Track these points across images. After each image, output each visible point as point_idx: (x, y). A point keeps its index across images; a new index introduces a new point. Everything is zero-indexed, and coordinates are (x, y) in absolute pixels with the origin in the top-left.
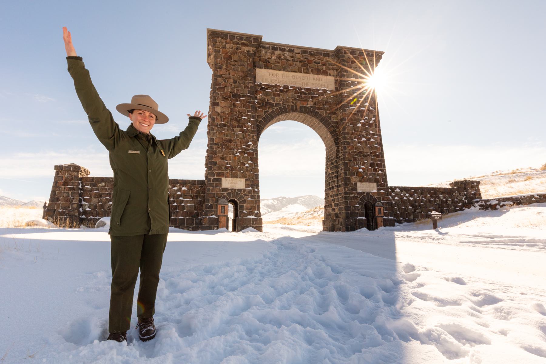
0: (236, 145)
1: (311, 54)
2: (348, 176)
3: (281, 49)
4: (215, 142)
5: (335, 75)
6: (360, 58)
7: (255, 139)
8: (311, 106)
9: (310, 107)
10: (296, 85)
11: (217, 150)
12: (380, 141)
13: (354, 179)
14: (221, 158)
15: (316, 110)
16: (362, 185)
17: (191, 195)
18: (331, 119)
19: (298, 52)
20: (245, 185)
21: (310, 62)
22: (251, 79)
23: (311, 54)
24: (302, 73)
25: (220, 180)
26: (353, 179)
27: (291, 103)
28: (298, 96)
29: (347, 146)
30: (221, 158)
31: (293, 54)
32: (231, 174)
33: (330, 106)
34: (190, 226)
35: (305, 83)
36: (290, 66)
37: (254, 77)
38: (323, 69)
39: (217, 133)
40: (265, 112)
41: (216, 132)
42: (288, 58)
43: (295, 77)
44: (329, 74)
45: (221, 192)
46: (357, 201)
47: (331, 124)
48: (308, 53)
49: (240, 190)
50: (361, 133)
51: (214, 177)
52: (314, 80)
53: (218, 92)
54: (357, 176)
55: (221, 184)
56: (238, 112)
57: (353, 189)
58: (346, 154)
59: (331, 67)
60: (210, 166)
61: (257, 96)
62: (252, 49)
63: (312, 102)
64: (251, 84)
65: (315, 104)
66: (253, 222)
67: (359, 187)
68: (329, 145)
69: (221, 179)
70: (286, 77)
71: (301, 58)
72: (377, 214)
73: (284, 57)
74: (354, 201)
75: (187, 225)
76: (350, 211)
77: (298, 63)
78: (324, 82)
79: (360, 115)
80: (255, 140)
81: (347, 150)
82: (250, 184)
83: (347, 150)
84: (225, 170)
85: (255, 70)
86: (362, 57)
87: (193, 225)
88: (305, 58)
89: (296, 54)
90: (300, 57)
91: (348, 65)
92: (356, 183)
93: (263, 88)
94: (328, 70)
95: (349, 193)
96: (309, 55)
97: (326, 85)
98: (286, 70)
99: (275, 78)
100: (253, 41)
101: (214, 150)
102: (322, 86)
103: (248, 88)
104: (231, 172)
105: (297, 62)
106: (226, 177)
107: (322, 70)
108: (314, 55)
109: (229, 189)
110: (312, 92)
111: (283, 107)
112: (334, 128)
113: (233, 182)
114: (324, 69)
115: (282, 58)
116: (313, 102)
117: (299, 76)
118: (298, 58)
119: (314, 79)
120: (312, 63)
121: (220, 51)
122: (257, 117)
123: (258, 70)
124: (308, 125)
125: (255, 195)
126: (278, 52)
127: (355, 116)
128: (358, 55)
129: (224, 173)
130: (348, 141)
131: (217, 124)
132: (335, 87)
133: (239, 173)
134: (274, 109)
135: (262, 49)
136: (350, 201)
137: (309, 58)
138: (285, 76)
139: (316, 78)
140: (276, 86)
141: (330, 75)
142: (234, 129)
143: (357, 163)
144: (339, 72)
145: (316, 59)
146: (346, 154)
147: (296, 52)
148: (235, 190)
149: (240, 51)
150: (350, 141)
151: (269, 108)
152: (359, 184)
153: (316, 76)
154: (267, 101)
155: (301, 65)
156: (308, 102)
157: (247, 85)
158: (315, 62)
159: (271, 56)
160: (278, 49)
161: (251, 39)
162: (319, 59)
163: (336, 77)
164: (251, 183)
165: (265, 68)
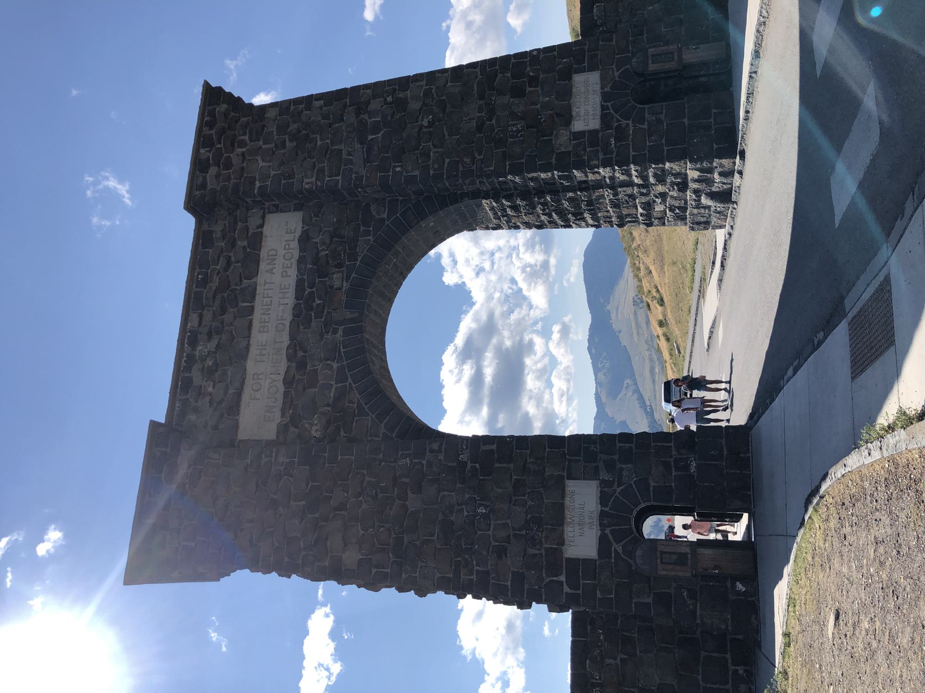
0: (459, 508)
1: (204, 283)
2: (553, 161)
3: (188, 369)
4: (451, 575)
5: (262, 211)
6: (219, 146)
7: (440, 447)
8: (345, 277)
9: (347, 282)
10: (284, 322)
11: (476, 568)
12: (444, 74)
13: (562, 140)
14: (500, 557)
15: (358, 263)
16: (578, 115)
17: (622, 660)
18: (383, 220)
20: (588, 479)
23: (204, 283)
24: (253, 308)
25: (574, 563)
26: (561, 145)
27: (338, 335)
29: (461, 169)
30: (500, 557)
31: (201, 333)
32: (549, 527)
34: (730, 673)
35: (281, 295)
36: (235, 341)
38: (244, 247)
39: (421, 567)
41: (418, 570)
42: (212, 345)
43: (264, 327)
44: (260, 230)
45: (613, 560)
46: (631, 128)
47: (397, 217)
48: (200, 290)
49: (604, 499)
50: (425, 130)
51: (563, 582)
52: (274, 271)
53: (301, 557)
54: (551, 134)
55: (584, 560)
58: (485, 169)
59: (240, 224)
60: (525, 595)
61: (315, 437)
65: (340, 266)
68: (457, 222)
69: (569, 560)
70: (263, 352)
71: (214, 308)
72: (672, 65)
73: (208, 359)
75: (727, 683)
76: (666, 148)
77: (227, 317)
79: (374, 137)
80: (443, 446)
81: (474, 168)
82: (584, 464)
84: (538, 547)
85: (241, 441)
88: (214, 298)
89: (204, 323)
91: (235, 179)
92: (574, 133)
96: (207, 287)
97: (291, 237)
101: (475, 579)
102: (289, 249)
104: (545, 527)
105: (223, 319)
106: (563, 544)
107: (248, 250)
109: (599, 533)
110: (305, 277)
111: (346, 361)
113: (576, 520)
115: (210, 363)
116: (333, 274)
117: (262, 314)
118: (214, 317)
119: (271, 271)
120: (228, 276)
122: (374, 438)
123: (243, 435)
124: (399, 285)
125: (620, 446)
126: (197, 377)
127: (376, 148)
128: (211, 150)
129: (547, 550)
130: (446, 166)
132: (295, 210)
133: (549, 501)
134: (354, 386)
136: (631, 148)
137: (214, 288)
138: (261, 355)
139: (267, 264)
140: (288, 382)
141: (262, 226)
142: (409, 512)
144: (252, 201)
145: (218, 267)
147: (196, 324)
148: (602, 515)
150: (447, 161)
152: (578, 126)
153: (263, 266)
154: (329, 409)
156: (335, 287)
158: (226, 270)
162: (219, 260)
163: (267, 211)
164: (579, 461)
165: (238, 414)
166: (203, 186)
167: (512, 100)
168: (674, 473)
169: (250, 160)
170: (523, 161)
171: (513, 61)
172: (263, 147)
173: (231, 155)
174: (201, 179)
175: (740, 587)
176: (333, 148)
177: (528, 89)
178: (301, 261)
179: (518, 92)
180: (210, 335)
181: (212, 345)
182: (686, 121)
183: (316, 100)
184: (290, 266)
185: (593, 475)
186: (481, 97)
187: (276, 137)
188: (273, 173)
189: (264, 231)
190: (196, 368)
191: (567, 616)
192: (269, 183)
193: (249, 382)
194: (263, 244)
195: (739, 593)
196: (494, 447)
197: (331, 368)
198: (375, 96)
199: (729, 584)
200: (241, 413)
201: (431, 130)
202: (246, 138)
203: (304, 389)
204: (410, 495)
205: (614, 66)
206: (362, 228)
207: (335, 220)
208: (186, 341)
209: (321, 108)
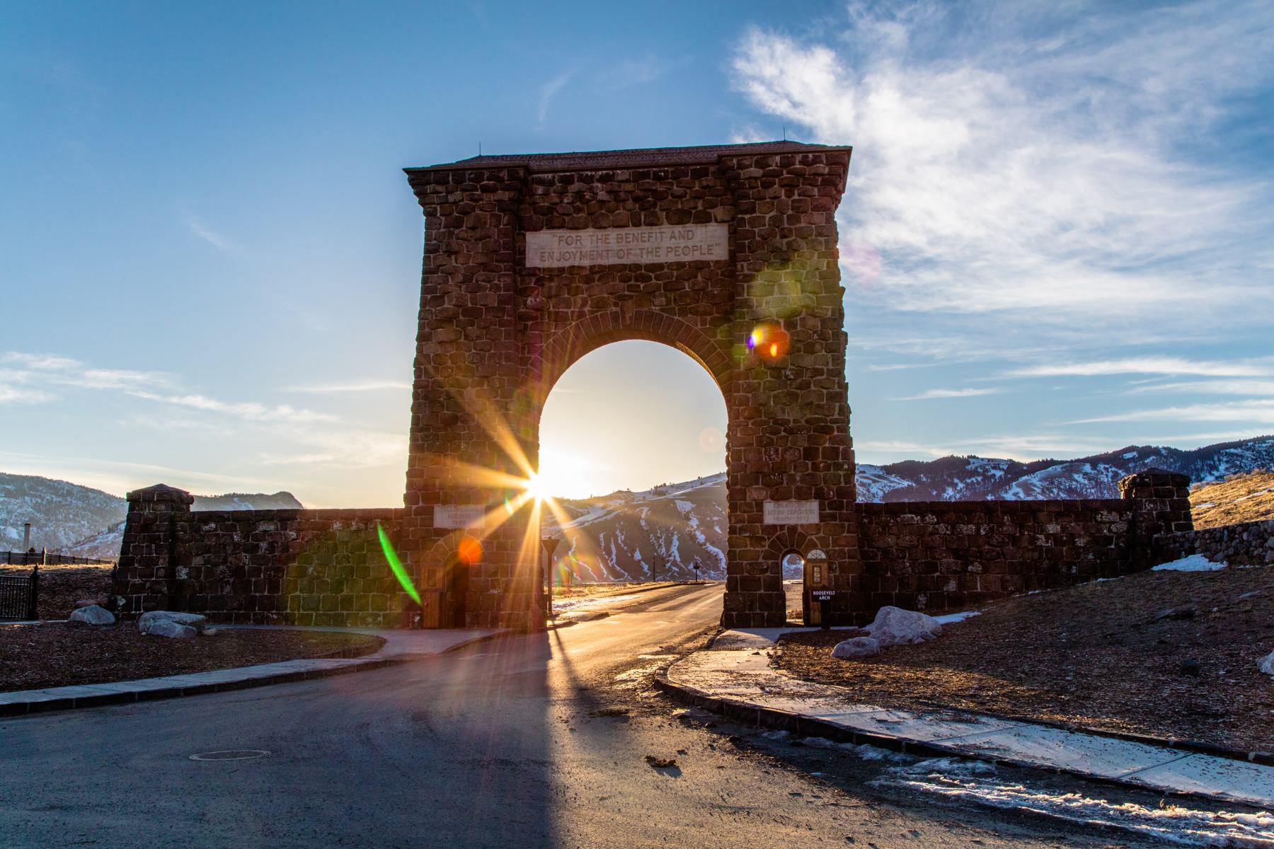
3: (581, 179)
5: (726, 218)
6: (785, 172)
9: (660, 310)
12: (836, 386)
13: (754, 494)
16: (779, 506)
21: (659, 196)
22: (505, 266)
23: (657, 178)
28: (628, 286)
29: (741, 408)
33: (712, 302)
37: (523, 252)
38: (695, 208)
42: (602, 195)
44: (713, 218)
46: (760, 549)
50: (783, 372)
51: (417, 503)
52: (673, 240)
56: (473, 351)
58: (739, 429)
62: (505, 196)
63: (664, 299)
69: (433, 508)
74: (752, 549)
76: (738, 576)
77: (630, 204)
78: (700, 241)
83: (741, 419)
85: (524, 236)
86: (788, 169)
87: (385, 610)
89: (623, 184)
90: (632, 189)
92: (762, 503)
94: (712, 208)
95: (740, 529)
97: (705, 247)
98: (598, 225)
99: (572, 249)
100: (506, 178)
103: (498, 288)
108: (666, 177)
110: (666, 270)
112: (724, 359)
114: (700, 208)
115: (587, 197)
120: (666, 198)
121: (435, 208)
131: (425, 383)
132: (730, 251)
135: (535, 186)
141: (716, 221)
143: (765, 452)
145: (675, 188)
146: (739, 429)
147: (620, 178)
149: (481, 202)
151: (556, 326)
152: (769, 506)
155: (637, 206)
157: (496, 282)
158: (672, 195)
159: (560, 197)
160: (576, 179)
161: (501, 175)
165: (548, 229)
166: (741, 167)
167: (802, 449)
168: (490, 579)
169: (773, 204)
170: (743, 462)
171: (841, 447)
172: (785, 216)
173: (776, 186)
174: (747, 162)
175: (417, 618)
176: (776, 287)
177: (810, 463)
178: (680, 265)
180: (610, 192)
181: (602, 195)
182: (762, 591)
183: (828, 264)
184: (677, 253)
186: (807, 421)
187: (793, 227)
188: (756, 230)
189: (711, 224)
191: (402, 505)
192: (747, 228)
193: (574, 234)
194: (699, 225)
195: (413, 618)
199: (418, 612)
200: (548, 231)
201: (783, 378)
202: (796, 197)
205: (821, 534)
206: (709, 318)
207: (716, 292)
208: (604, 172)
209: (817, 269)
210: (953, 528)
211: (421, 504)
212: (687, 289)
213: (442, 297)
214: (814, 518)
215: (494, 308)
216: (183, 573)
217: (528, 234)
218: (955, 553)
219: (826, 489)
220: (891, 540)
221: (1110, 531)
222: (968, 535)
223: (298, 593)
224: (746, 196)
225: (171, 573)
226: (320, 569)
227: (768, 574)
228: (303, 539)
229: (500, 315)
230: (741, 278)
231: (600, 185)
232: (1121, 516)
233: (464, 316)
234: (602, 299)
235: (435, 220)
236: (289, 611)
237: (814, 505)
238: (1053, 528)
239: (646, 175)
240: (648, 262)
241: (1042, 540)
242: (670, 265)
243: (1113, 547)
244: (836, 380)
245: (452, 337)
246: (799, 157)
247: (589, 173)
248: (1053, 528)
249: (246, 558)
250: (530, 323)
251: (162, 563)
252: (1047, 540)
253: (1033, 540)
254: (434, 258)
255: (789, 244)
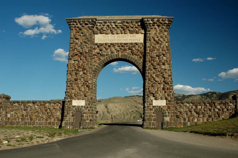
3: (109, 22)
15: (131, 56)
18: (141, 61)
19: (119, 23)
21: (128, 27)
23: (127, 23)
25: (71, 101)
37: (94, 39)
40: (100, 59)
42: (114, 26)
49: (82, 107)
57: (150, 104)
64: (90, 45)
66: (88, 124)
67: (154, 103)
69: (72, 101)
77: (120, 28)
85: (94, 35)
88: (124, 25)
93: (99, 45)
97: (138, 40)
100: (91, 21)
103: (88, 47)
118: (120, 26)
129: (73, 97)
135: (97, 23)
141: (141, 33)
147: (118, 22)
152: (154, 101)
154: (101, 53)
158: (131, 27)
166: (148, 21)
171: (171, 88)
174: (149, 19)
176: (156, 49)
178: (132, 44)
179: (163, 89)
180: (116, 26)
181: (114, 26)
182: (153, 121)
183: (168, 44)
185: (86, 104)
188: (151, 36)
190: (109, 24)
193: (107, 35)
196: (91, 87)
197: (109, 52)
198: (167, 58)
203: (105, 47)
204: (82, 72)
208: (114, 21)
209: (165, 45)
210: (196, 107)
211: (69, 100)
212: (134, 49)
213: (75, 49)
214: (165, 105)
215: (87, 52)
216: (9, 116)
217: (95, 35)
218: (197, 113)
219: (168, 97)
220: (182, 110)
221: (231, 108)
222: (200, 109)
223: (37, 121)
224: (149, 28)
225: (6, 116)
226: (43, 115)
227: (154, 117)
228: (39, 108)
229: (89, 54)
230: (147, 47)
231: (113, 24)
232: (233, 104)
233: (80, 54)
234: (114, 51)
235: (73, 31)
236: (35, 125)
237: (165, 101)
238: (219, 107)
239: (124, 22)
240: (125, 42)
241: (217, 110)
242: (130, 43)
243: (231, 111)
244: (170, 71)
245: (77, 59)
246: (161, 19)
247: (111, 21)
248: (219, 107)
249: (24, 113)
250: (96, 56)
251: (4, 113)
252: (217, 109)
253: (214, 110)
254: (73, 40)
255: (159, 39)
